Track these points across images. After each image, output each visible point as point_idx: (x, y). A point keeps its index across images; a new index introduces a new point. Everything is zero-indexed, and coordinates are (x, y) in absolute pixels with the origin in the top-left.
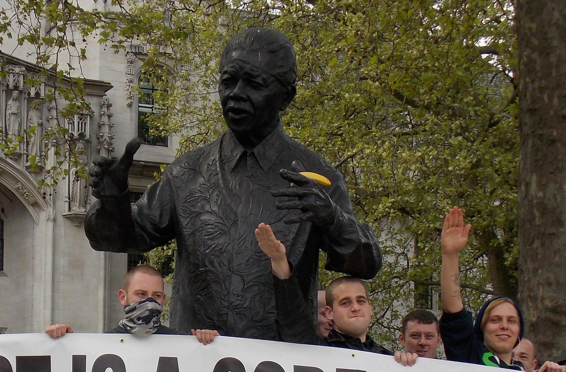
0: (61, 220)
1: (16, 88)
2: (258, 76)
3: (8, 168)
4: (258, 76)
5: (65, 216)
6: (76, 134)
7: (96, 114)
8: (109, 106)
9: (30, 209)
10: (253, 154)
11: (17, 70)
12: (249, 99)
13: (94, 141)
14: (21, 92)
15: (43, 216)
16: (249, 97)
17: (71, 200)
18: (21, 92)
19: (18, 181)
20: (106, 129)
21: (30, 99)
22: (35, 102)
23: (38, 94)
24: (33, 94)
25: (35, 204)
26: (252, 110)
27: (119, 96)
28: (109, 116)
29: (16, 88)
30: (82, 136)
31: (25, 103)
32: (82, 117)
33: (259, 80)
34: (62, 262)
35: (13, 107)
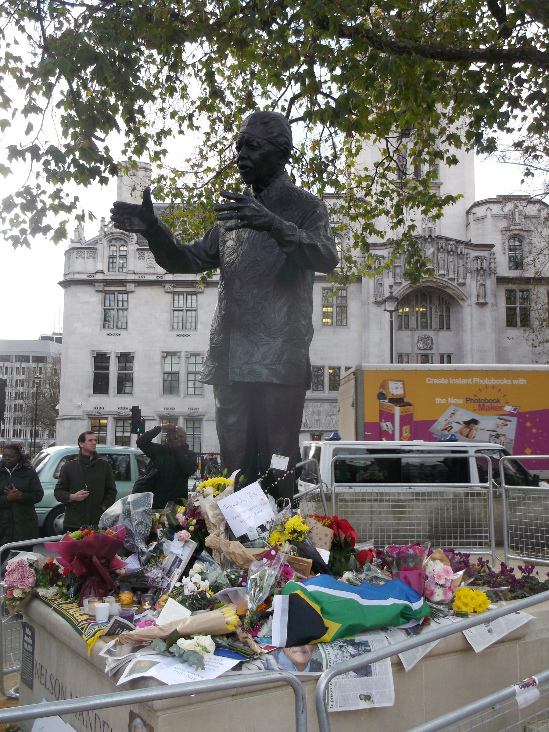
0: (474, 305)
1: (452, 250)
2: (253, 141)
3: (449, 285)
4: (253, 141)
5: (476, 304)
6: (479, 268)
7: (488, 258)
8: (494, 254)
9: (461, 302)
10: (260, 197)
11: (452, 243)
12: (249, 158)
13: (488, 270)
14: (454, 252)
15: (466, 304)
16: (249, 156)
17: (478, 296)
18: (454, 252)
19: (454, 290)
20: (493, 265)
21: (458, 255)
22: (461, 255)
23: (461, 252)
24: (459, 252)
25: (462, 299)
26: (253, 166)
27: (498, 249)
28: (494, 259)
29: (452, 250)
30: (482, 268)
31: (456, 257)
32: (482, 260)
33: (255, 144)
34: (475, 323)
35: (451, 259)
